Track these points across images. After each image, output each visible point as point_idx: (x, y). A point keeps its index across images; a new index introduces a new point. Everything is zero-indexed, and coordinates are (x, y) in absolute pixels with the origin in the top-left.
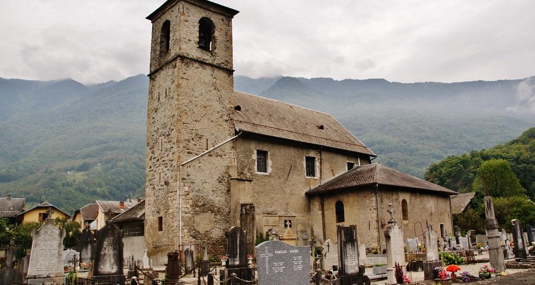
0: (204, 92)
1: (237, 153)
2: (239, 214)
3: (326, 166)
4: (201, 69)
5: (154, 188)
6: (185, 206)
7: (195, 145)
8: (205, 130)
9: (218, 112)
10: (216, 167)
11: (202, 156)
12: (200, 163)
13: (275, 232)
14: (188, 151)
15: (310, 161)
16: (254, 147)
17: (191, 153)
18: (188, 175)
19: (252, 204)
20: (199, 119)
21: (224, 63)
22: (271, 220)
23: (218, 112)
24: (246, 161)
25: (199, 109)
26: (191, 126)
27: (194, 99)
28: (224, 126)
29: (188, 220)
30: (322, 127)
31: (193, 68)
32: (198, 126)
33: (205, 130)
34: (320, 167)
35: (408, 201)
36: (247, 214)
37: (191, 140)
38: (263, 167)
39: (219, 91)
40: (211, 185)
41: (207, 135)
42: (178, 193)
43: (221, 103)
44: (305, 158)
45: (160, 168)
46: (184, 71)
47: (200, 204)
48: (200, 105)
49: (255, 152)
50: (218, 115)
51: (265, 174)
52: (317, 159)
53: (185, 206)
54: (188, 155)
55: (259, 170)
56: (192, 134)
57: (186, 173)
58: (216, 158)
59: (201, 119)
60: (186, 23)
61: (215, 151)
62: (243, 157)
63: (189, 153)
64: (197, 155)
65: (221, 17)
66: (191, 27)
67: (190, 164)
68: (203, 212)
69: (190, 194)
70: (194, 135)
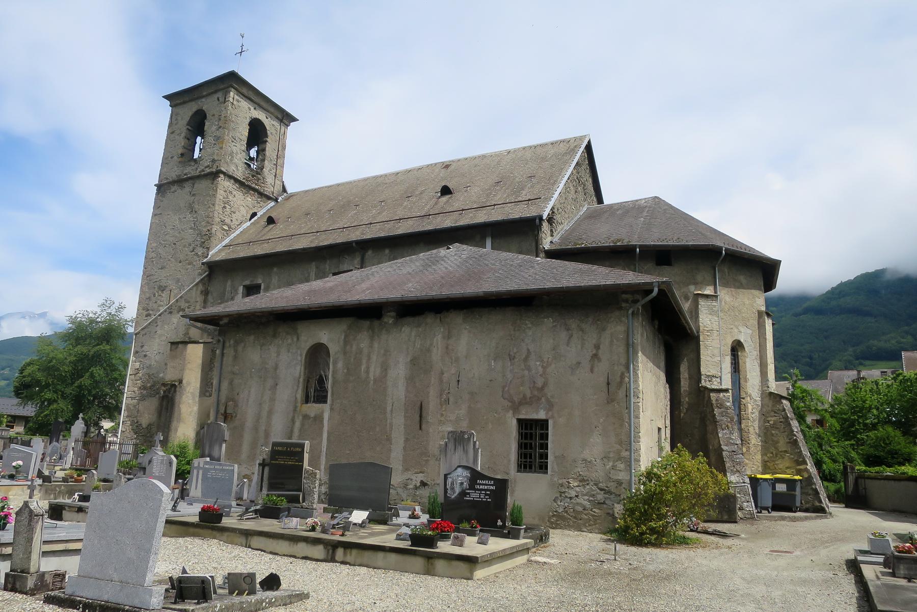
9: (190, 245)
18: (142, 347)
21: (208, 166)
35: (333, 348)
41: (171, 284)
53: (132, 389)
61: (179, 304)
63: (147, 316)
67: (146, 330)
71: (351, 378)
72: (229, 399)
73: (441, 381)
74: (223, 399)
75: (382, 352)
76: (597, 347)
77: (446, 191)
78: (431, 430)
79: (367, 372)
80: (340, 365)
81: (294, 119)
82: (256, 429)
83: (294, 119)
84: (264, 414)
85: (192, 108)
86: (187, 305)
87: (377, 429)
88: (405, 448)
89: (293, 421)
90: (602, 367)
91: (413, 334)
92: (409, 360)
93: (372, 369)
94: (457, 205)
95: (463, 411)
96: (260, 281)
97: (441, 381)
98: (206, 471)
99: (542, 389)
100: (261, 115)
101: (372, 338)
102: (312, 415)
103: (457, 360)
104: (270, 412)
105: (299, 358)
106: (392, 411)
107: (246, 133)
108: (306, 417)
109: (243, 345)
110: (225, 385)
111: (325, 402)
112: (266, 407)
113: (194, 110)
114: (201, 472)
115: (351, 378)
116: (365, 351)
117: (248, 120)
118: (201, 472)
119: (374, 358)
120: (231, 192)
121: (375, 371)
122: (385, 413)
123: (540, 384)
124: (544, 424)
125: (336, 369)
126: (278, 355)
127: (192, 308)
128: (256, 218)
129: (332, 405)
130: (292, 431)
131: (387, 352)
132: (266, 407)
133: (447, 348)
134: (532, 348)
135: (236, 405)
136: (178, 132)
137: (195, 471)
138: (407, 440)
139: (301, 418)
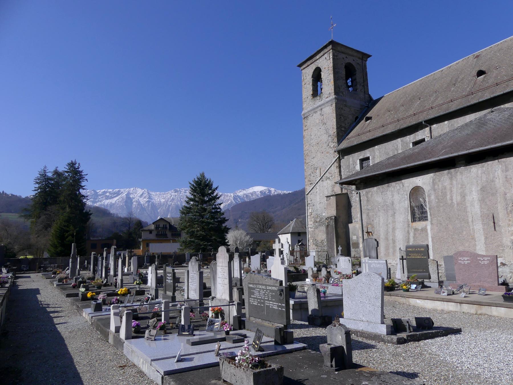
35: (427, 188)
50: (325, 145)
62: (348, 172)
72: (368, 224)
75: (460, 186)
77: (480, 73)
78: (503, 231)
80: (433, 197)
81: (369, 56)
82: (387, 239)
83: (369, 56)
84: (390, 230)
85: (313, 67)
87: (464, 233)
88: (485, 243)
89: (408, 232)
91: (480, 172)
92: (479, 189)
93: (454, 197)
94: (491, 81)
96: (368, 155)
98: (370, 265)
100: (350, 60)
101: (451, 179)
102: (420, 228)
104: (394, 229)
106: (472, 221)
107: (344, 73)
108: (416, 230)
109: (371, 193)
111: (427, 220)
112: (391, 226)
113: (314, 68)
114: (367, 265)
115: (442, 204)
116: (448, 187)
117: (344, 65)
118: (367, 265)
119: (454, 190)
120: (342, 109)
121: (457, 198)
122: (468, 223)
125: (430, 200)
126: (393, 196)
128: (358, 119)
129: (431, 221)
130: (409, 238)
132: (391, 226)
133: (506, 178)
136: (308, 83)
137: (364, 264)
138: (486, 238)
139: (413, 230)
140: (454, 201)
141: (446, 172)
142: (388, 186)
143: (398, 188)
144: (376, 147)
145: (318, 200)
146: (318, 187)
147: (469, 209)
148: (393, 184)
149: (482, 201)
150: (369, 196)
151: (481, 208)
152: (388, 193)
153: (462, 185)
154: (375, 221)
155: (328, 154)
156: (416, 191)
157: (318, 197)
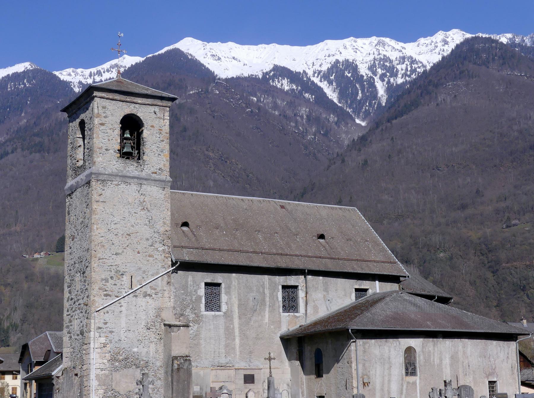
0: (127, 214)
1: (175, 289)
2: (170, 369)
3: (317, 296)
4: (123, 186)
5: (71, 337)
6: (100, 361)
7: (115, 285)
8: (128, 265)
9: (147, 239)
10: (144, 309)
11: (124, 297)
12: (121, 306)
13: (228, 390)
14: (105, 293)
15: (290, 290)
16: (198, 281)
17: (110, 296)
18: (106, 323)
19: (189, 357)
20: (120, 251)
21: (156, 173)
22: (223, 374)
23: (147, 239)
24: (188, 298)
25: (120, 238)
26: (109, 262)
27: (113, 226)
28: (156, 257)
29: (104, 378)
30: (322, 237)
31: (112, 186)
32: (118, 260)
33: (128, 265)
34: (305, 298)
35: (418, 350)
36: (178, 369)
37: (110, 279)
38: (212, 303)
39: (149, 211)
40: (137, 334)
42: (92, 345)
43: (151, 227)
44: (280, 287)
45: (76, 312)
46: (100, 192)
47: (121, 358)
48: (122, 233)
49: (203, 285)
51: (217, 313)
52: (300, 288)
53: (100, 361)
54: (105, 298)
55: (207, 310)
56: (111, 271)
57: (103, 321)
58: (144, 299)
59: (123, 252)
60: (102, 127)
61: (144, 289)
62: (183, 294)
63: (106, 295)
64: (117, 297)
65: (152, 109)
66: (109, 131)
68: (125, 367)
69: (108, 346)
70: (113, 273)
71: (427, 364)
72: (363, 375)
73: (463, 366)
74: (360, 374)
76: (508, 354)
79: (434, 361)
80: (422, 357)
82: (382, 390)
84: (386, 382)
86: (153, 291)
89: (402, 385)
90: (510, 361)
93: (435, 360)
95: (471, 379)
96: (219, 281)
97: (463, 366)
99: (494, 369)
101: (434, 346)
102: (411, 382)
103: (467, 357)
104: (389, 381)
105: (401, 354)
108: (408, 383)
109: (368, 345)
110: (360, 366)
112: (386, 378)
115: (427, 364)
116: (432, 351)
119: (436, 355)
121: (437, 361)
123: (494, 368)
124: (495, 382)
125: (420, 360)
126: (390, 352)
127: (160, 295)
129: (420, 377)
130: (402, 390)
131: (441, 353)
132: (386, 378)
134: (490, 353)
135: (369, 378)
140: (435, 363)
141: (431, 339)
142: (386, 341)
143: (395, 345)
144: (234, 275)
145: (123, 325)
146: (125, 305)
147: (444, 370)
148: (391, 340)
149: (451, 365)
150: (367, 347)
151: (451, 370)
152: (385, 347)
153: (441, 352)
154: (371, 373)
155: (151, 258)
156: (409, 351)
157: (123, 320)
